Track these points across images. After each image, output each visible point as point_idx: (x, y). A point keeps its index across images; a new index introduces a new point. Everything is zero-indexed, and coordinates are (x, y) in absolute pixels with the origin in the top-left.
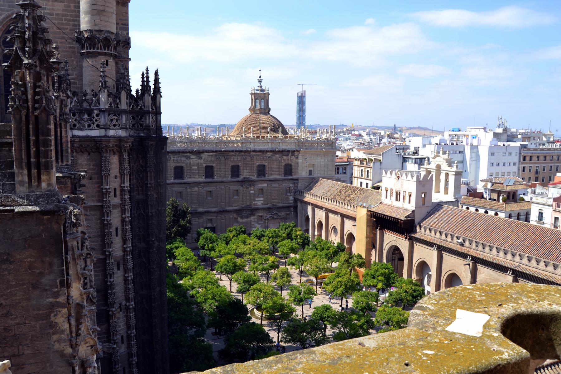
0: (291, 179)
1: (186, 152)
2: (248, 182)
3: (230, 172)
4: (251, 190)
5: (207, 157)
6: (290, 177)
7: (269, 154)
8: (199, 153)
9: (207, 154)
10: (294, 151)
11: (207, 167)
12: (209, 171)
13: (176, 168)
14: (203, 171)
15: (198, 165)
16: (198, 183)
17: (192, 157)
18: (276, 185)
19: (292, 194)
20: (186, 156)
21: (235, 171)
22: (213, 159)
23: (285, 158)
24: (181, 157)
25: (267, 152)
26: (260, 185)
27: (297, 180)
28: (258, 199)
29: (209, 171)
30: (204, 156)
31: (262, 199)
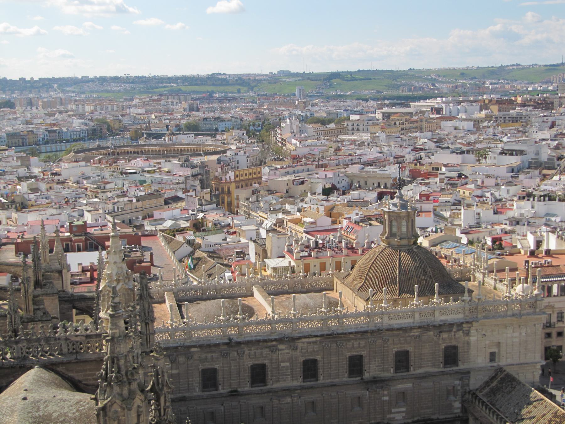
0: (457, 373)
1: (272, 341)
2: (377, 382)
3: (346, 367)
4: (384, 396)
5: (305, 345)
6: (455, 368)
7: (416, 333)
8: (291, 340)
9: (307, 340)
10: (462, 323)
11: (306, 363)
12: (310, 369)
13: (253, 367)
14: (299, 369)
15: (290, 360)
16: (289, 391)
17: (281, 347)
18: (428, 384)
19: (459, 397)
20: (270, 347)
21: (356, 365)
22: (316, 347)
23: (445, 335)
24: (262, 349)
25: (412, 328)
26: (400, 386)
27: (467, 373)
28: (396, 410)
29: (310, 369)
30: (300, 344)
31: (404, 409)
